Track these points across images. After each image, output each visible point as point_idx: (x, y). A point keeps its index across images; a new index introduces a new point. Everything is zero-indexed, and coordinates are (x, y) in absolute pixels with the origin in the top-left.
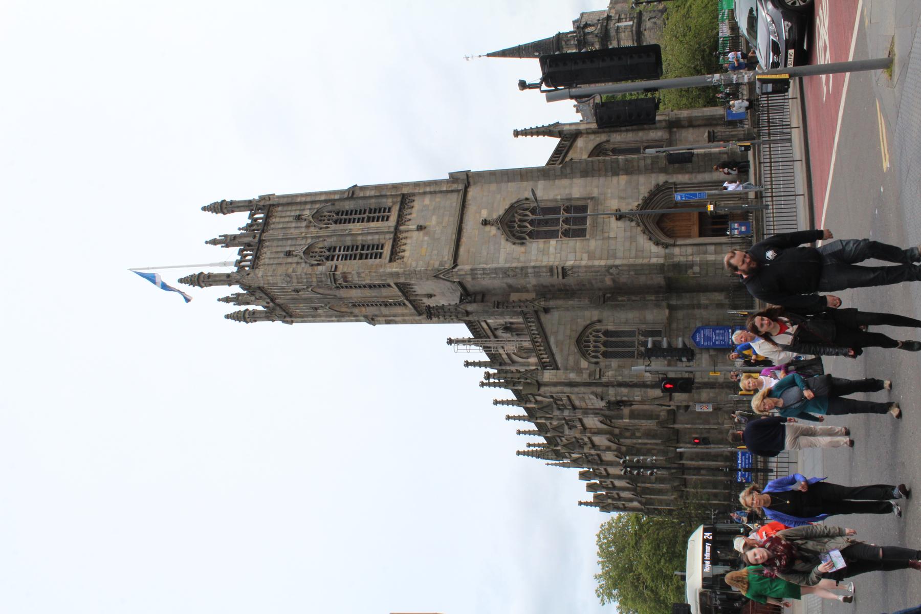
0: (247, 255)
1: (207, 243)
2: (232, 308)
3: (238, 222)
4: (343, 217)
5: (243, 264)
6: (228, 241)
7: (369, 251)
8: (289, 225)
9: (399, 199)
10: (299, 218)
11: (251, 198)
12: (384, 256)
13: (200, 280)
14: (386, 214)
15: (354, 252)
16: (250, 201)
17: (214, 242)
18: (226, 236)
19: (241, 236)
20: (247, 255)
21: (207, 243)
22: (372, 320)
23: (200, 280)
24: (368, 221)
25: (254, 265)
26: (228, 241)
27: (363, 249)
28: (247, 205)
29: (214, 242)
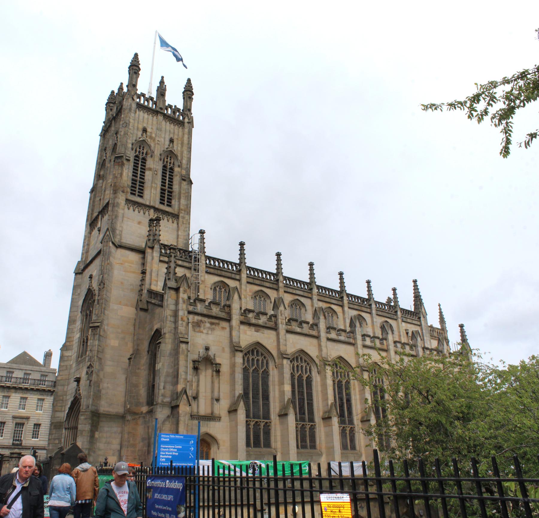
0: (148, 102)
1: (163, 77)
2: (116, 91)
3: (174, 98)
4: (168, 173)
5: (142, 98)
6: (162, 90)
7: (138, 186)
8: (168, 133)
9: (176, 213)
10: (172, 141)
11: (192, 111)
12: (132, 196)
13: (134, 68)
14: (166, 203)
15: (139, 176)
16: (190, 110)
17: (162, 82)
18: (165, 90)
19: (164, 101)
20: (148, 102)
21: (163, 77)
22: (92, 191)
23: (134, 68)
24: (162, 189)
25: (140, 106)
26: (162, 90)
27: (140, 182)
28: (187, 109)
29: (162, 82)
